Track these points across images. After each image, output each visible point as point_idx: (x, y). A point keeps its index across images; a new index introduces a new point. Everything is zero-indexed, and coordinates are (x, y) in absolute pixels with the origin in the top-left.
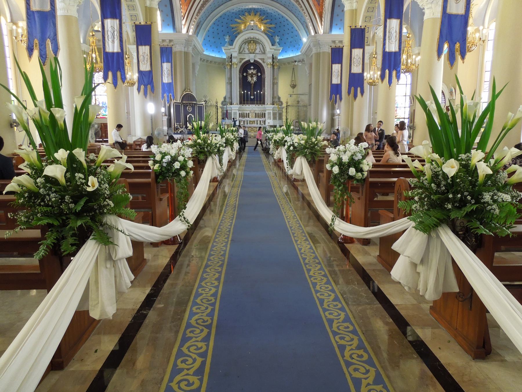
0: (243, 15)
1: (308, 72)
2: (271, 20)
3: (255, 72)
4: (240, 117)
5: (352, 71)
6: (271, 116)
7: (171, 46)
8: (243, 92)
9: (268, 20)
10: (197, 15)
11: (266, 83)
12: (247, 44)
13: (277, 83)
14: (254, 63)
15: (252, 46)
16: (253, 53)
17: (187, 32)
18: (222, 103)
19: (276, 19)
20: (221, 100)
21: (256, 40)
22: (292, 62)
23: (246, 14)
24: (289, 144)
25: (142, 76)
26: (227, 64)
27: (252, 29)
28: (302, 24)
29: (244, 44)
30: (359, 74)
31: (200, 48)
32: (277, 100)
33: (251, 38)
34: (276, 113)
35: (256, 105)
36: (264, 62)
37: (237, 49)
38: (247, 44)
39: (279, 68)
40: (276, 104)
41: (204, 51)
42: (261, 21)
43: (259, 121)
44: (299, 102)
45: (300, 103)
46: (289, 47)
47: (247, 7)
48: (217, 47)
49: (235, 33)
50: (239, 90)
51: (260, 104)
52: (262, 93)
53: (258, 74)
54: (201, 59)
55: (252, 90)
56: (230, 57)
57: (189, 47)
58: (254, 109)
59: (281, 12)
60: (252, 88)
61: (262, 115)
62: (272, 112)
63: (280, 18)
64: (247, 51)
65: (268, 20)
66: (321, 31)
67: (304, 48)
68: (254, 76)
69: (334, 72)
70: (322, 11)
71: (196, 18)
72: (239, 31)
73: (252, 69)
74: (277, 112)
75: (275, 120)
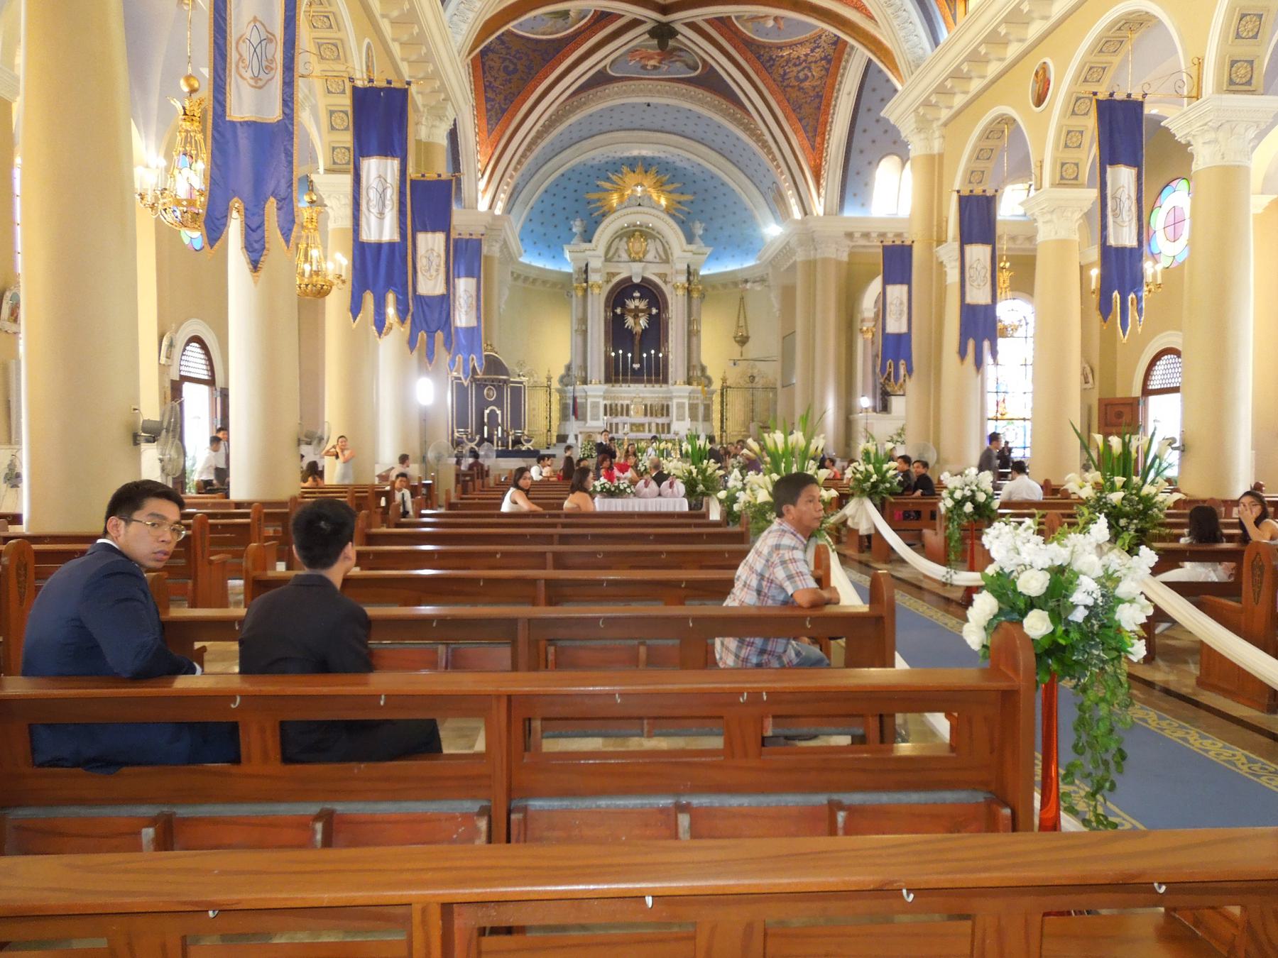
0: (616, 171)
2: (684, 184)
4: (605, 415)
5: (969, 300)
6: (684, 412)
7: (480, 237)
8: (613, 354)
9: (679, 185)
10: (515, 169)
12: (625, 239)
13: (698, 332)
14: (642, 284)
15: (637, 245)
16: (640, 261)
17: (490, 207)
18: (562, 380)
19: (695, 182)
21: (647, 230)
22: (735, 284)
23: (625, 169)
24: (958, 495)
25: (423, 311)
26: (577, 287)
27: (639, 205)
28: (763, 194)
29: (617, 240)
30: (986, 307)
31: (513, 244)
32: (699, 374)
33: (634, 226)
34: (697, 404)
35: (648, 385)
36: (665, 282)
37: (601, 251)
38: (625, 239)
39: (703, 296)
40: (695, 383)
41: (521, 256)
42: (660, 186)
43: (653, 426)
44: (754, 377)
45: (757, 379)
46: (725, 248)
47: (627, 154)
48: (549, 247)
49: (596, 214)
50: (603, 349)
51: (657, 381)
52: (661, 355)
53: (651, 311)
54: (512, 273)
55: (637, 349)
56: (584, 269)
57: (494, 244)
58: (641, 395)
59: (713, 167)
60: (637, 342)
61: (662, 409)
62: (686, 401)
63: (704, 180)
64: (624, 256)
65: (677, 185)
66: (818, 208)
67: (770, 253)
68: (640, 314)
69: (891, 304)
70: (821, 164)
71: (511, 177)
72: (606, 209)
73: (637, 298)
74: (699, 401)
75: (695, 423)
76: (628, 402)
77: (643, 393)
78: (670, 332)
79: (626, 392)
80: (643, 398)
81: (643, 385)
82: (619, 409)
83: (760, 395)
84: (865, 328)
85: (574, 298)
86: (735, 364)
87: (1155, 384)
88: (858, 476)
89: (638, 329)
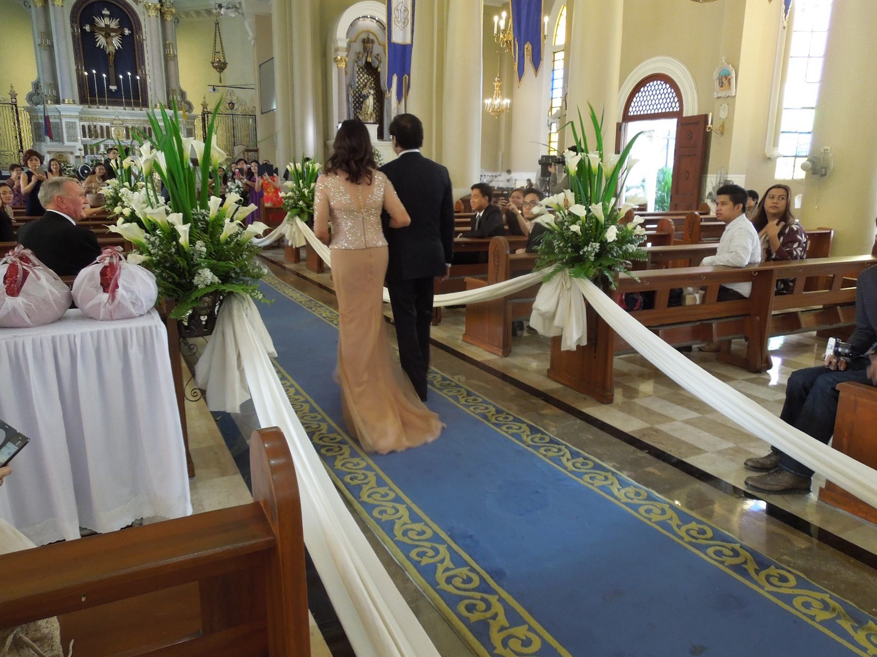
1: (251, 34)
3: (114, 24)
4: (84, 136)
11: (148, 56)
13: (175, 56)
18: (30, 98)
20: (24, 89)
32: (179, 98)
35: (127, 108)
44: (233, 104)
50: (74, 67)
51: (137, 105)
60: (111, 63)
61: (145, 131)
68: (112, 34)
76: (108, 124)
77: (123, 115)
78: (146, 56)
79: (106, 114)
80: (123, 121)
81: (122, 108)
82: (99, 131)
83: (238, 120)
84: (339, 57)
85: (33, 8)
86: (214, 90)
87: (632, 112)
88: (576, 228)
89: (110, 49)
